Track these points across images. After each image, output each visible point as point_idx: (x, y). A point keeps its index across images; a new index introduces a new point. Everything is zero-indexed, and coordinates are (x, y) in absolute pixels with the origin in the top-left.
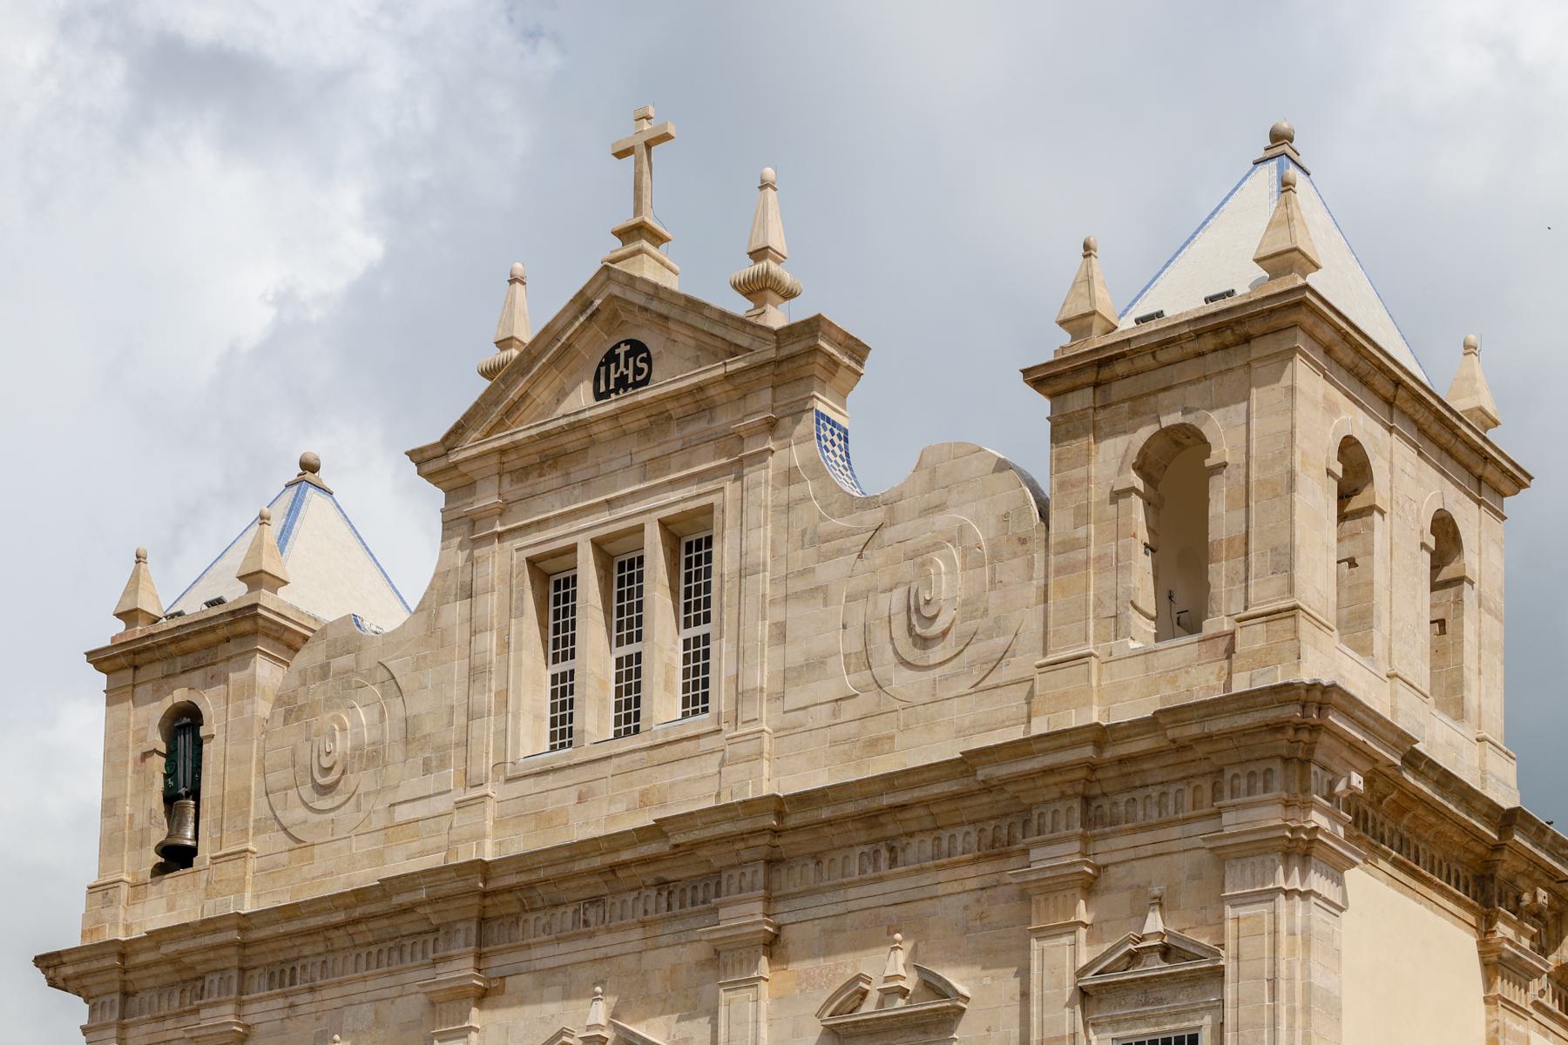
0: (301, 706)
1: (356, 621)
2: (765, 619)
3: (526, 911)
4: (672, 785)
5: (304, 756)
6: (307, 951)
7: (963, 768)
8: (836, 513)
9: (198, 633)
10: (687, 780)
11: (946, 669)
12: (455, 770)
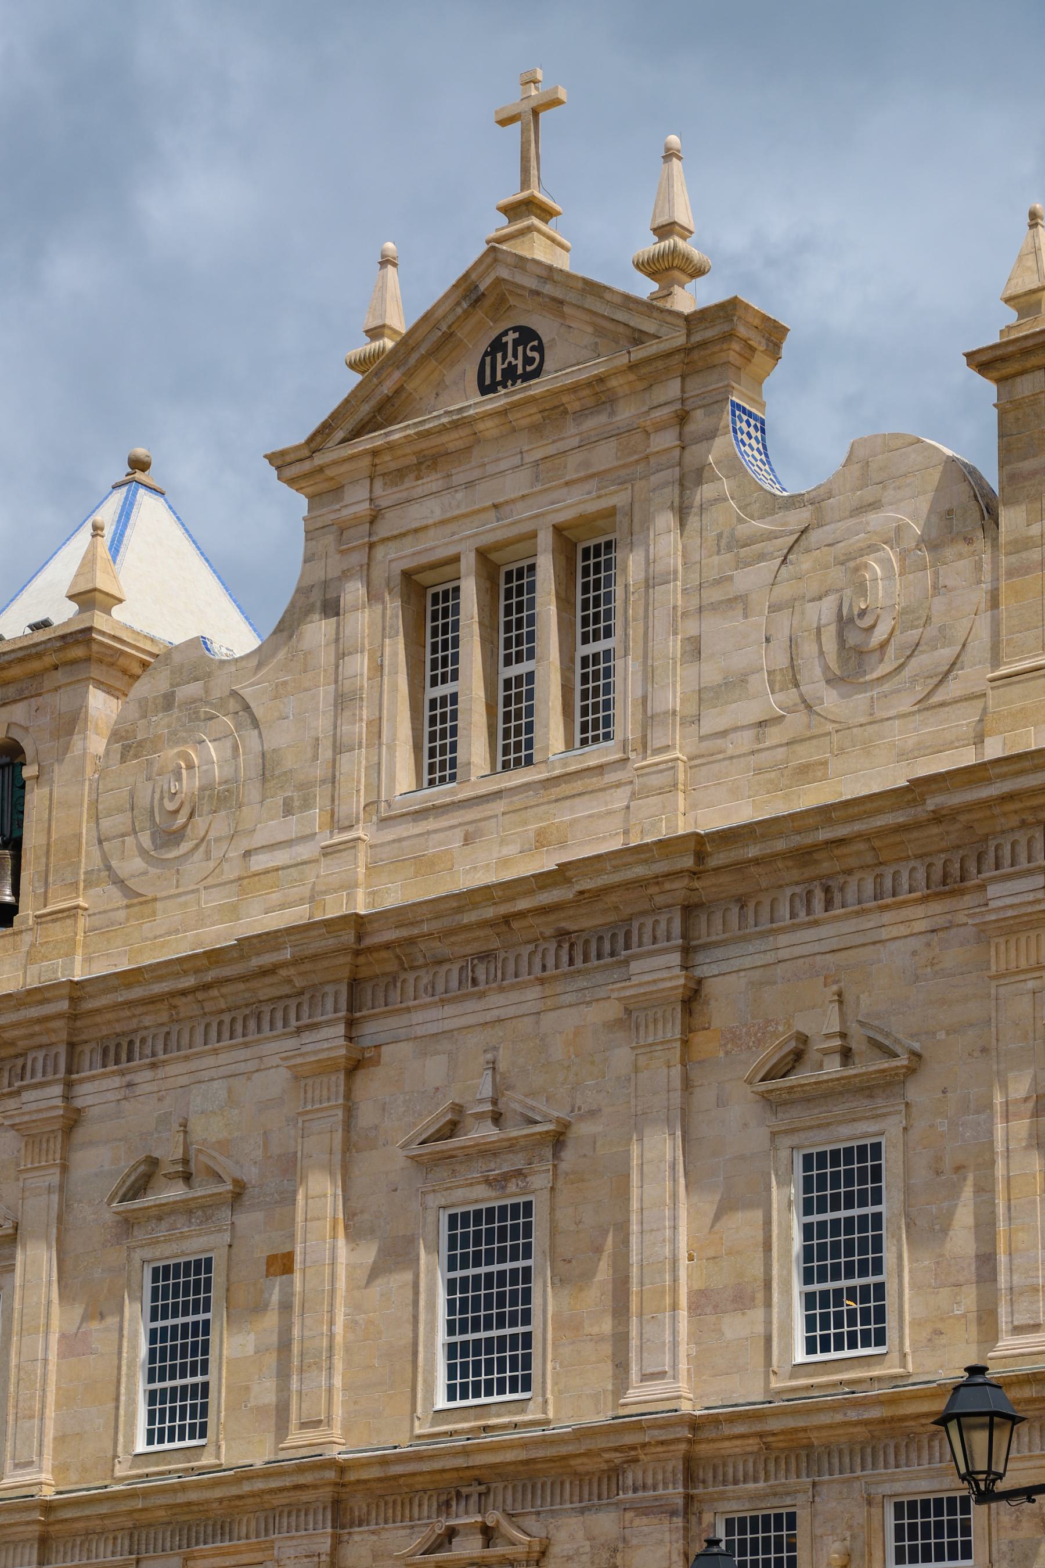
0: (141, 741)
1: (205, 643)
2: (677, 634)
3: (405, 970)
4: (573, 823)
5: (144, 798)
6: (148, 1021)
7: (910, 797)
8: (756, 514)
9: (21, 660)
10: (590, 816)
11: (886, 687)
12: (320, 810)
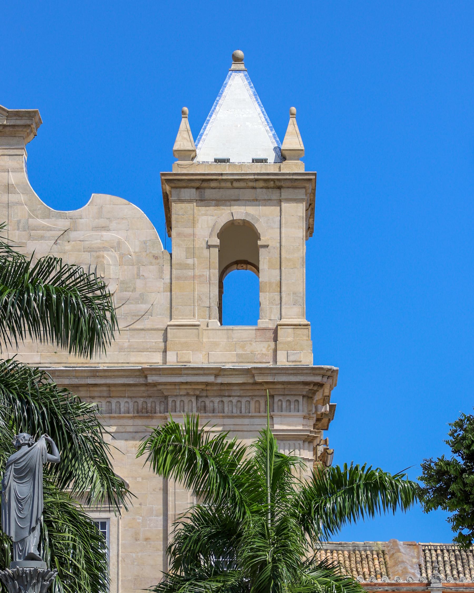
8: (39, 216)
